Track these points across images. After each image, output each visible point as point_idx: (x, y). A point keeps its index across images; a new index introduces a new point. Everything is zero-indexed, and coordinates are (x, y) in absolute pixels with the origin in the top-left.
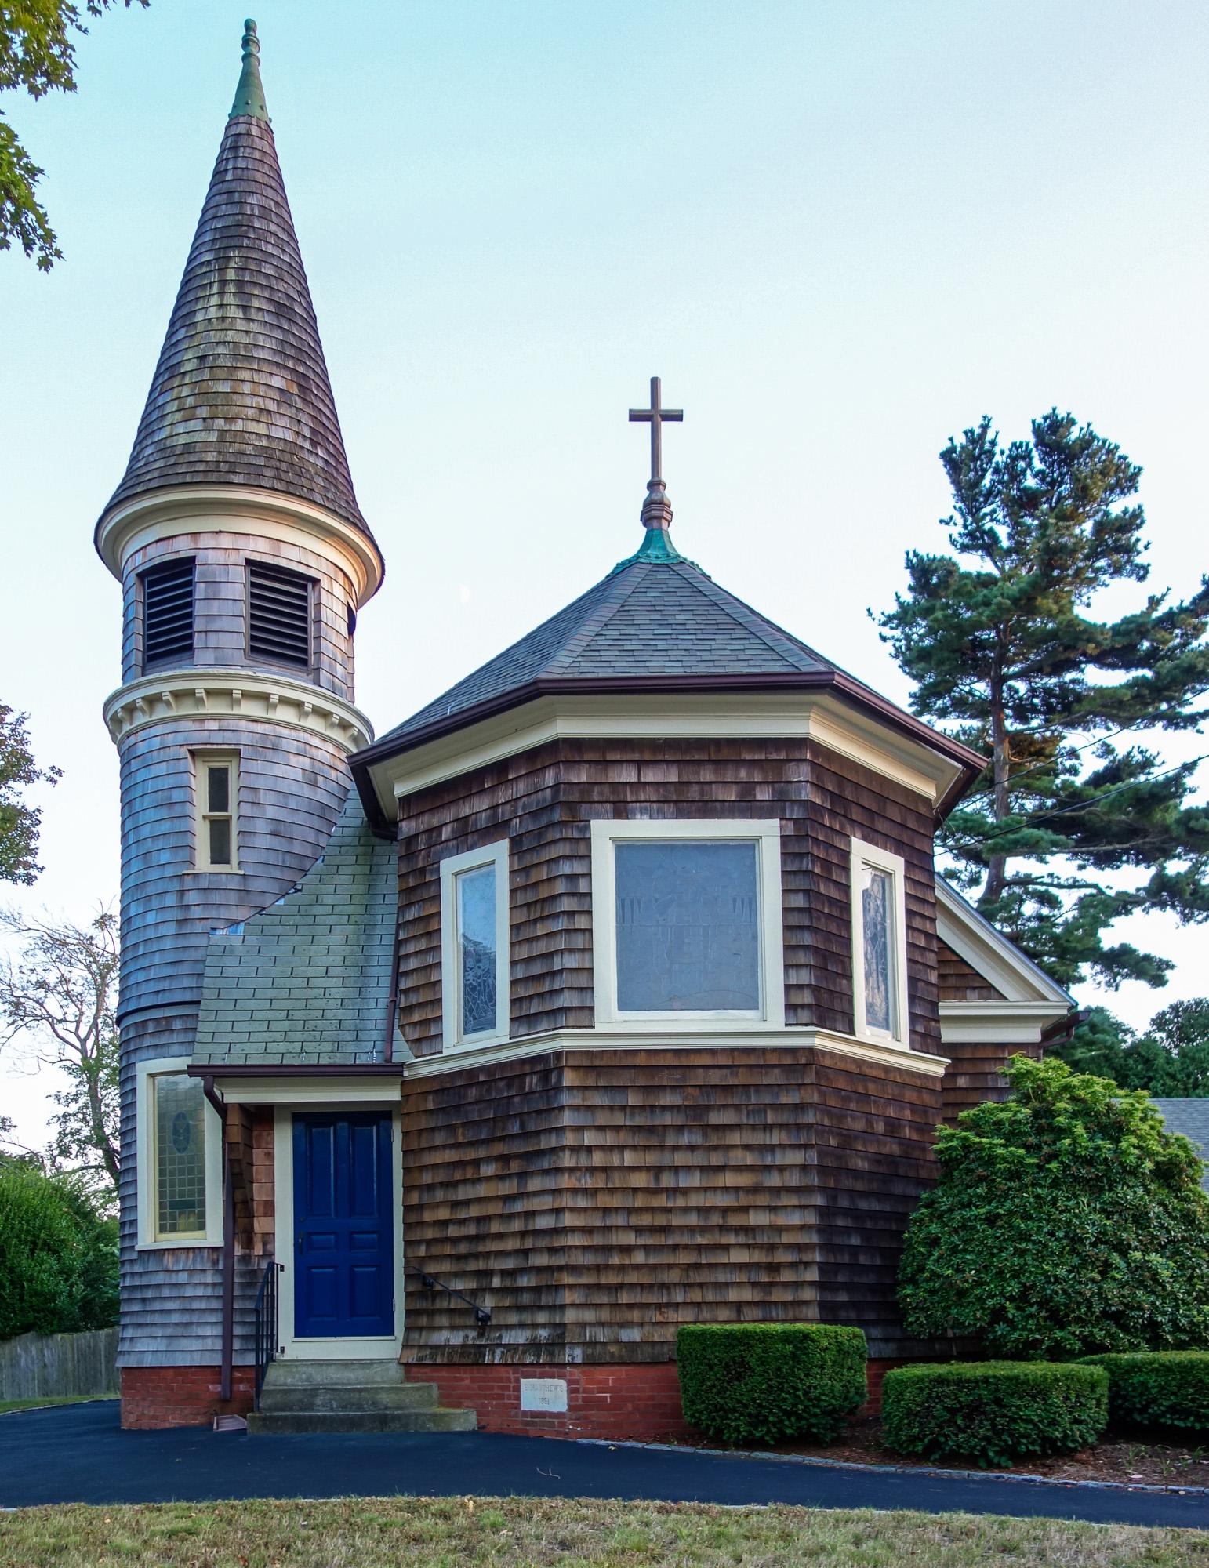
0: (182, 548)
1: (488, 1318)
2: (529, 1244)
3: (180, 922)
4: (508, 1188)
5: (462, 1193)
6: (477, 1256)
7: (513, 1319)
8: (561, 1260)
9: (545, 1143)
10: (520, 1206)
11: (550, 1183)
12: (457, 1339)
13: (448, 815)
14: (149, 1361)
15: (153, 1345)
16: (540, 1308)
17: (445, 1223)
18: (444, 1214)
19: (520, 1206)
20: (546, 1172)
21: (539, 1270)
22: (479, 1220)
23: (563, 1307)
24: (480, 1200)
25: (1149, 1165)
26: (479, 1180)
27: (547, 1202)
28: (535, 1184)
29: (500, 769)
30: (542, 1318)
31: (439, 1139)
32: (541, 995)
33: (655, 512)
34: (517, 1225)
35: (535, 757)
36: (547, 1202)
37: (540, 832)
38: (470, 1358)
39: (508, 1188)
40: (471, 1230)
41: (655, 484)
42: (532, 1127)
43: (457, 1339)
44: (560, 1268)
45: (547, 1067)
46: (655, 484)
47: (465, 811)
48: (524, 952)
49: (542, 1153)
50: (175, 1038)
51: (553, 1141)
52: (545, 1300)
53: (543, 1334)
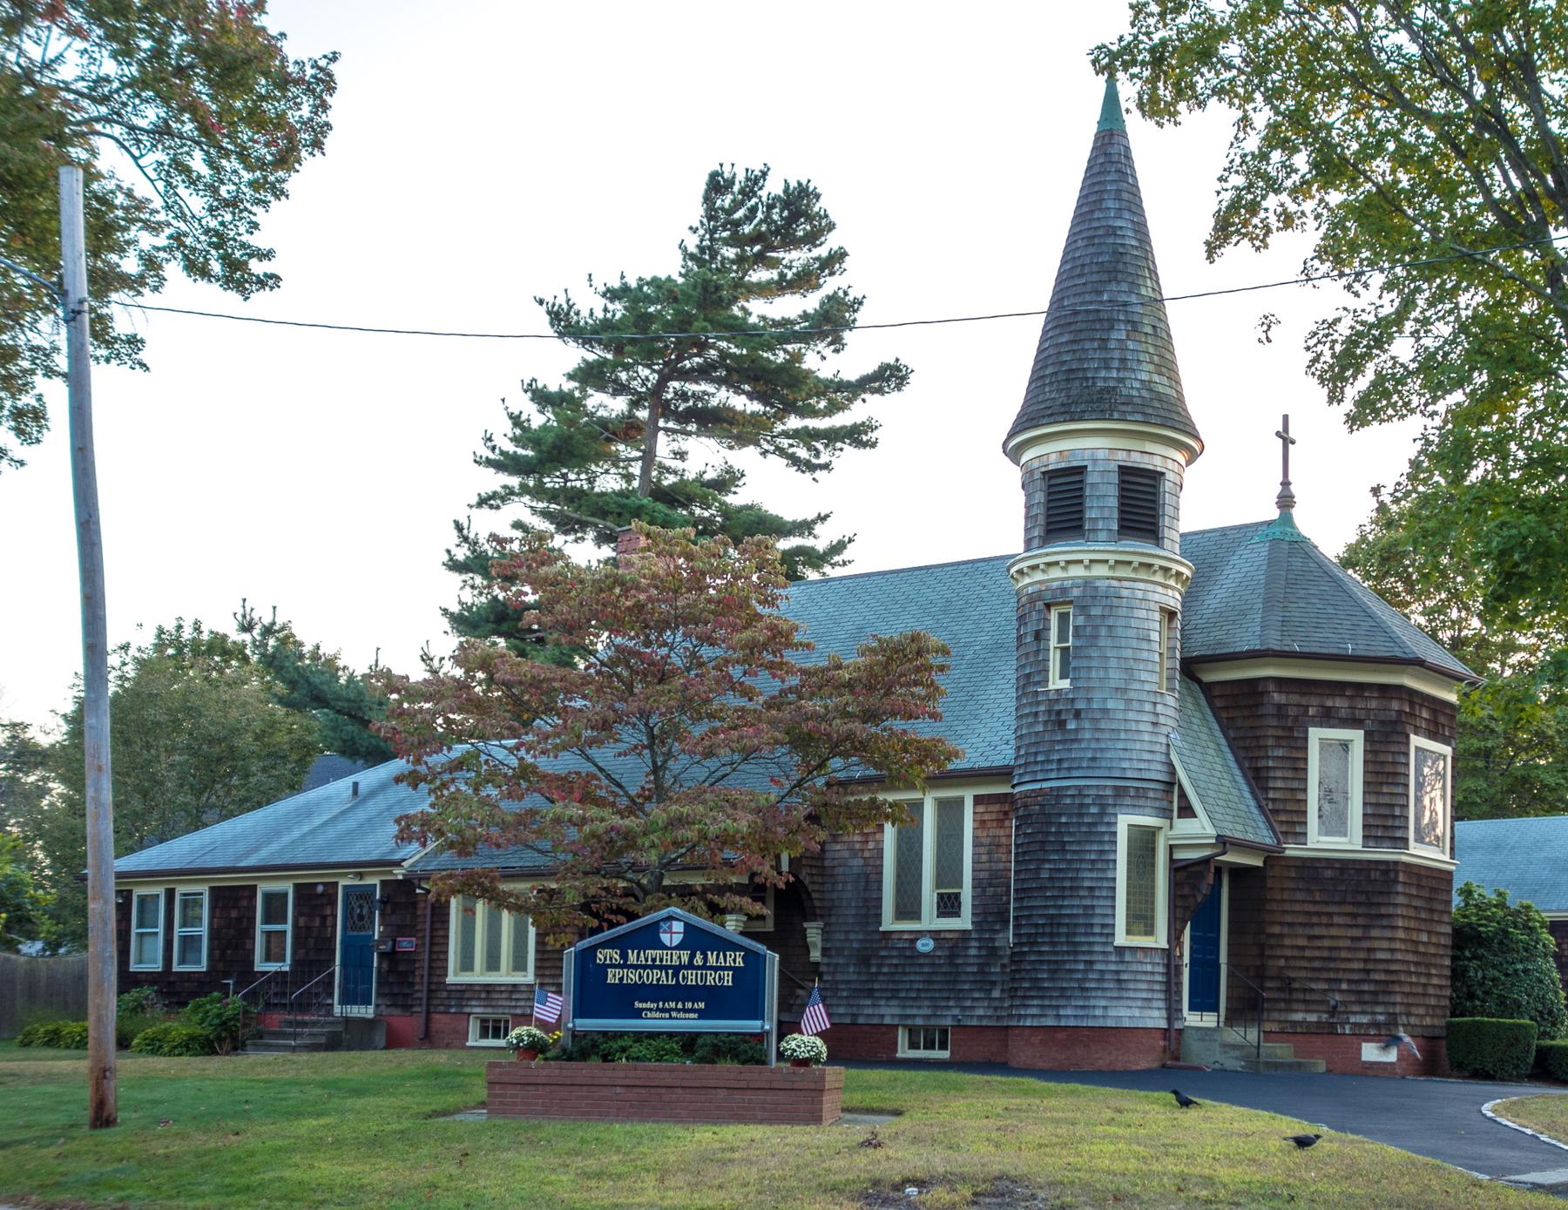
0: (1156, 463)
1: (1335, 1007)
2: (1370, 966)
3: (1155, 724)
4: (1357, 933)
5: (1317, 931)
6: (1328, 970)
7: (1356, 1008)
8: (1393, 978)
9: (1383, 911)
10: (1365, 944)
11: (1388, 934)
12: (1313, 1018)
13: (1315, 701)
14: (1126, 1023)
15: (1128, 1013)
16: (1378, 1003)
17: (1303, 948)
18: (1302, 942)
19: (1365, 944)
20: (1384, 927)
21: (1377, 982)
22: (1331, 949)
23: (1394, 1004)
24: (1332, 937)
25: (996, 994)
26: (1332, 925)
27: (1385, 944)
28: (1375, 933)
29: (1360, 687)
30: (1379, 1009)
31: (1300, 896)
32: (1385, 827)
33: (1286, 501)
34: (1362, 955)
35: (1384, 689)
36: (1385, 944)
37: (1387, 734)
38: (1327, 1030)
39: (1357, 933)
40: (1326, 954)
41: (1286, 484)
42: (1375, 900)
43: (1313, 1018)
44: (1393, 982)
45: (1390, 868)
46: (1286, 484)
47: (1329, 703)
48: (1373, 799)
49: (1383, 916)
50: (1149, 803)
51: (1391, 910)
52: (1381, 999)
53: (1381, 1018)
